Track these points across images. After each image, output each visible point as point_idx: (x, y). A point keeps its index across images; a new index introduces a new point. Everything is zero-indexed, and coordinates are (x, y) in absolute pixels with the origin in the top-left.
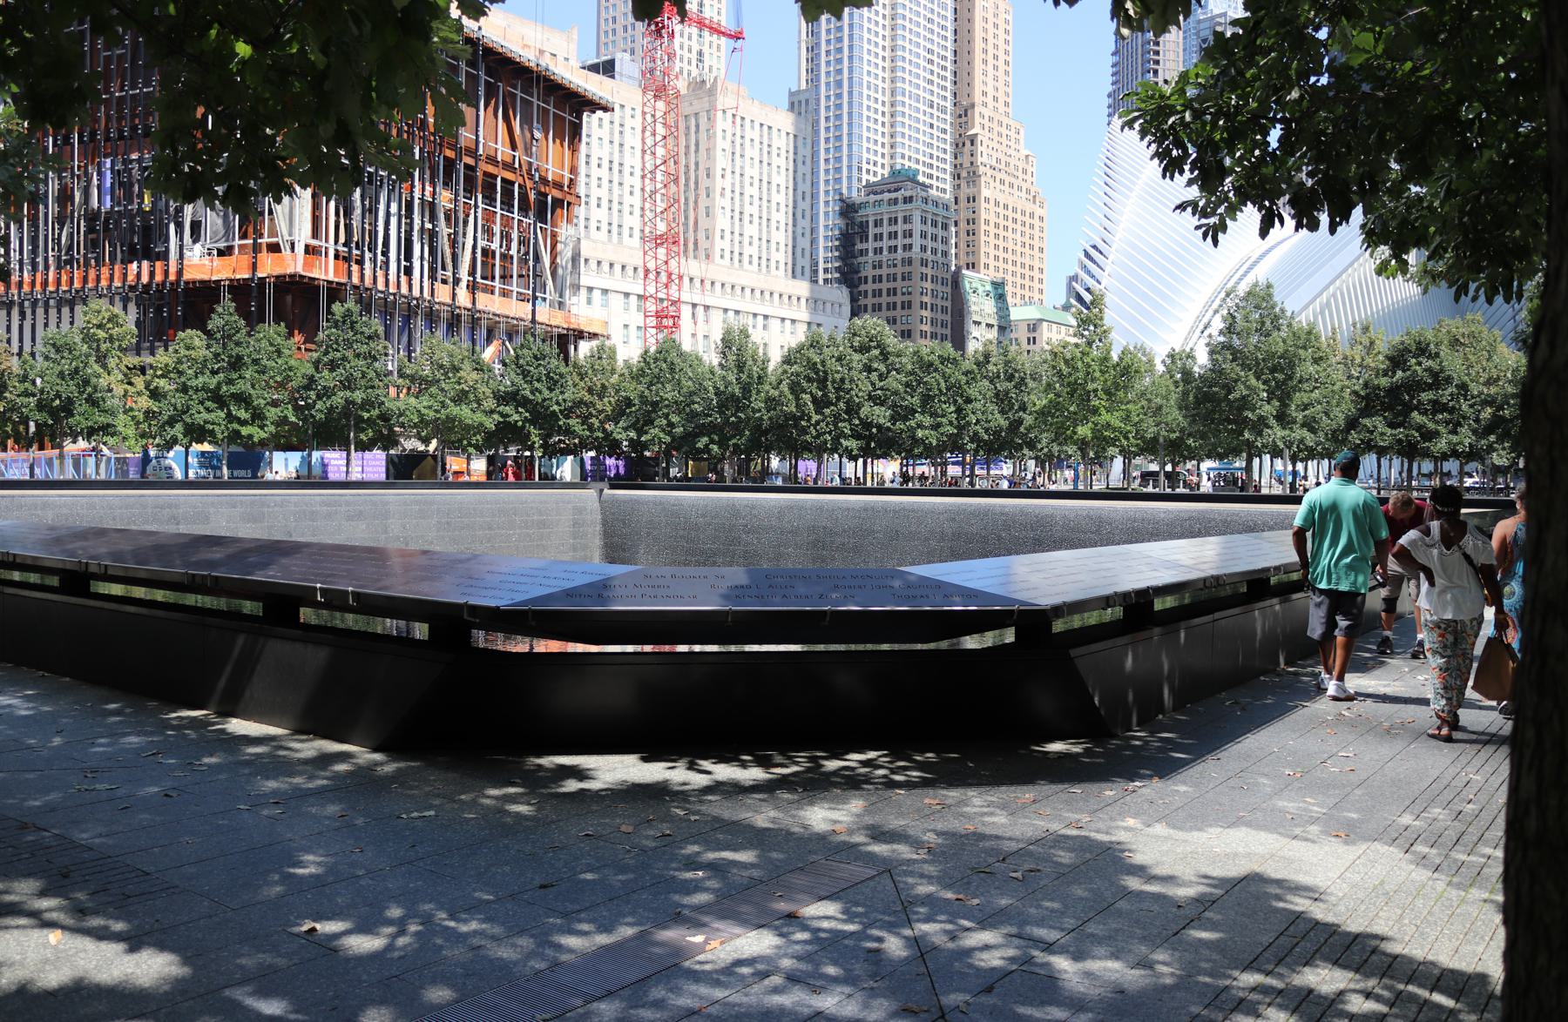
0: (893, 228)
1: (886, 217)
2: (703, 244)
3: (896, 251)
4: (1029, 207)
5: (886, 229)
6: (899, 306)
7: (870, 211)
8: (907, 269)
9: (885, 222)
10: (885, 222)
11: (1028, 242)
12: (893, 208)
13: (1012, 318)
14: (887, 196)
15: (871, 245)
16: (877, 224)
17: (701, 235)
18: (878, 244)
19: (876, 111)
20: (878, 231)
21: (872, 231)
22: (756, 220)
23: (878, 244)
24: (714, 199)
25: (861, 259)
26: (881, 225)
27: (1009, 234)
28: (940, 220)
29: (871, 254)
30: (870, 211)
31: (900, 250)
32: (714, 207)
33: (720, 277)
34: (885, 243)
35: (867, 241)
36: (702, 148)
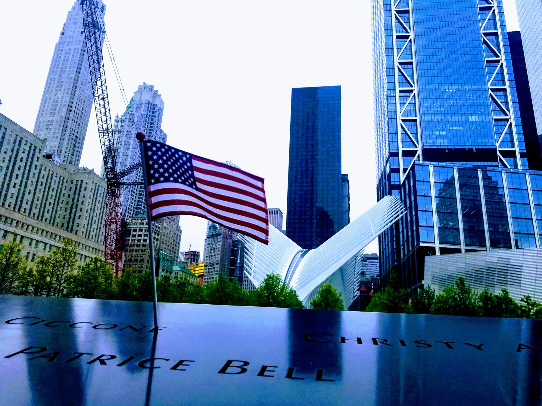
0: (140, 233)
1: (138, 229)
2: (75, 228)
3: (134, 241)
4: (177, 232)
5: (137, 233)
6: (139, 260)
7: (133, 226)
8: (144, 248)
9: (138, 230)
10: (138, 230)
11: (175, 244)
12: (142, 226)
13: (174, 269)
14: (140, 221)
15: (131, 238)
16: (135, 230)
17: (75, 225)
18: (134, 238)
19: (134, 192)
20: (134, 233)
21: (132, 233)
22: (97, 223)
23: (134, 238)
24: (84, 212)
25: (127, 243)
26: (142, 231)
27: (170, 241)
28: (157, 232)
29: (130, 241)
30: (133, 226)
31: (142, 241)
32: (83, 215)
33: (83, 242)
34: (136, 238)
35: (130, 236)
36: (82, 193)
